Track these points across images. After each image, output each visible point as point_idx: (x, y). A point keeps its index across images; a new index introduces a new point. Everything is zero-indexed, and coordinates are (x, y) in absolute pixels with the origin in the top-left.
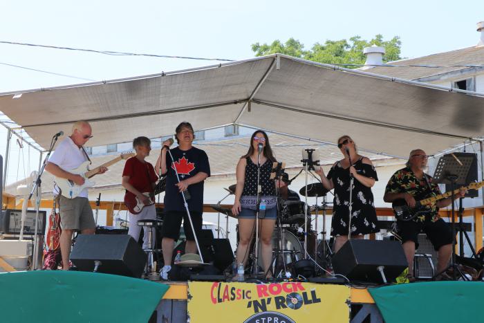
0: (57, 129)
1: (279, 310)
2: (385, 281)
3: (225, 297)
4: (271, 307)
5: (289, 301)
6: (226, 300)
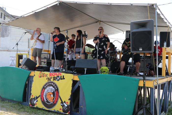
2: (85, 73)
3: (42, 76)
4: (52, 80)
5: (57, 78)
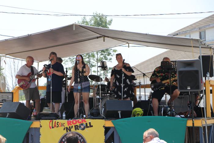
1: (76, 131)
2: (120, 117)
3: (55, 126)
4: (73, 130)
5: (80, 127)
6: (55, 127)
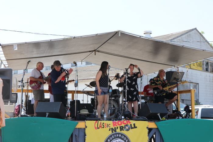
0: (28, 60)
1: (121, 132)
3: (100, 127)
4: (118, 131)
5: (125, 128)
6: (100, 128)
